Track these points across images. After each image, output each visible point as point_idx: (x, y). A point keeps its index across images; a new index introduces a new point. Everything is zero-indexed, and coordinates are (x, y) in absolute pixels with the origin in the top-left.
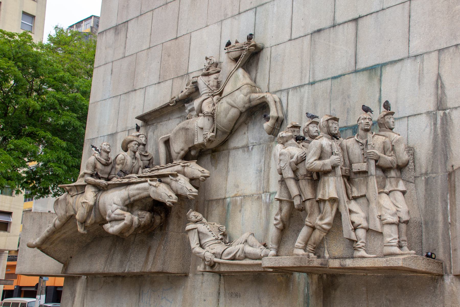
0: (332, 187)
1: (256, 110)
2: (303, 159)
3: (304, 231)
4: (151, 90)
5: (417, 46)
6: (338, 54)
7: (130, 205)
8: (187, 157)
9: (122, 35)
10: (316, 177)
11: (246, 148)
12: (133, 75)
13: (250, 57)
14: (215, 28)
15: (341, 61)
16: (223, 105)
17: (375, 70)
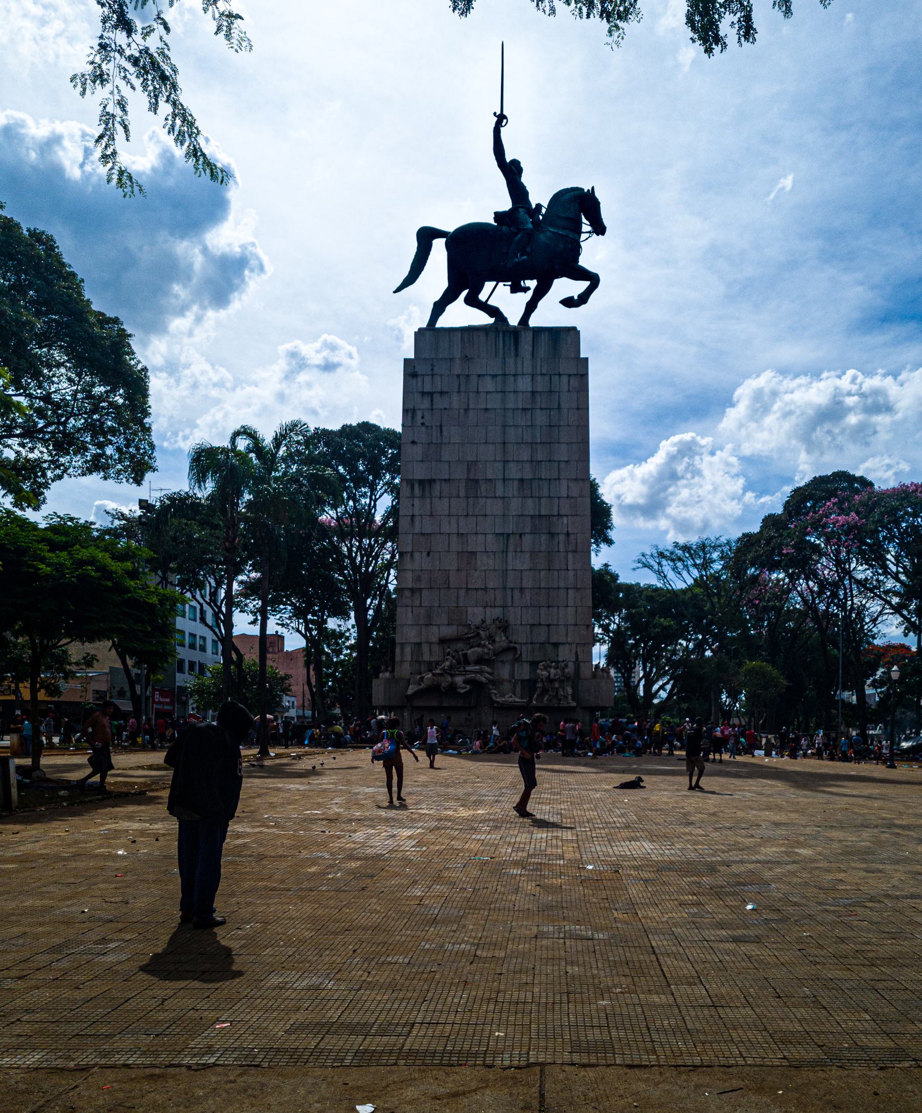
0: (557, 685)
1: (510, 649)
2: (549, 676)
3: (547, 697)
4: (443, 628)
5: (570, 640)
6: (541, 635)
7: (465, 682)
8: (477, 662)
9: (417, 595)
10: (551, 681)
11: (502, 662)
12: (429, 617)
13: (504, 626)
14: (481, 609)
15: (543, 639)
16: (497, 645)
17: (556, 645)
